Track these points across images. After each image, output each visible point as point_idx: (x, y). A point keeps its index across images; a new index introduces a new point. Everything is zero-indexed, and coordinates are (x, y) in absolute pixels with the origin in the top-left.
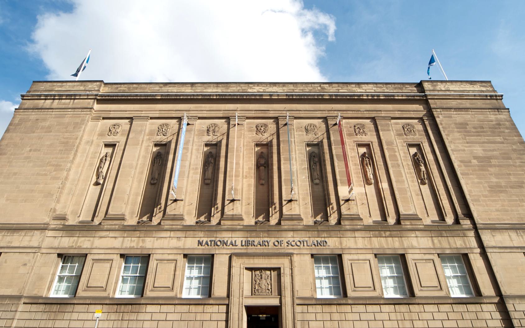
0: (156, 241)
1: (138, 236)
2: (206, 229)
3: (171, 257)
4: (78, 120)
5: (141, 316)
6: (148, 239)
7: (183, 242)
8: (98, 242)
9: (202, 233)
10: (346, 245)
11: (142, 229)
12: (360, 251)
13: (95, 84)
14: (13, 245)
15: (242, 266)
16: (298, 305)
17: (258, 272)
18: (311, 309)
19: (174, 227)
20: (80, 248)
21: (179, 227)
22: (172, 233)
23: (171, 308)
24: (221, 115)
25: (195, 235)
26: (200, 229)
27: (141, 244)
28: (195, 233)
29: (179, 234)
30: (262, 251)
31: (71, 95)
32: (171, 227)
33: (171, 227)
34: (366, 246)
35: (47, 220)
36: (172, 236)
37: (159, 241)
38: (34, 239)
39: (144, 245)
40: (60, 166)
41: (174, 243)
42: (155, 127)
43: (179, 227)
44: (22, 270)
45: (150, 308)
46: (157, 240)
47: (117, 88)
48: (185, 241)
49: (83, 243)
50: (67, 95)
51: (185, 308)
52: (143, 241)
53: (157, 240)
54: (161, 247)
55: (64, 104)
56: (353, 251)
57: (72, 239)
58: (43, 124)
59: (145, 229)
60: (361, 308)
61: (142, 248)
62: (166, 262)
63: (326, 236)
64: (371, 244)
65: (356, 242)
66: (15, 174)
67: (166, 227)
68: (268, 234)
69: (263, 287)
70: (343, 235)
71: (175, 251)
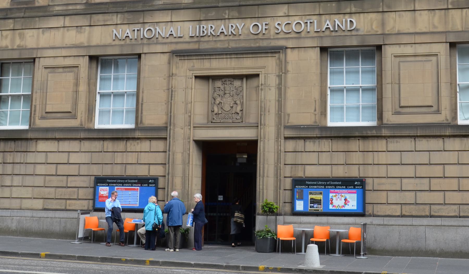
0: (41, 34)
1: (11, 27)
2: (126, 9)
5: (31, 158)
6: (29, 33)
7: (87, 32)
9: (119, 16)
10: (394, 27)
11: (17, 15)
12: (418, 39)
15: (190, 74)
16: (286, 138)
17: (218, 84)
18: (310, 146)
19: (70, 7)
21: (78, 7)
22: (67, 18)
23: (74, 146)
25: (107, 21)
26: (114, 10)
27: (18, 42)
28: (107, 17)
30: (226, 46)
32: (65, 8)
33: (65, 8)
34: (435, 27)
36: (67, 24)
37: (47, 34)
39: (22, 43)
41: (72, 37)
43: (78, 7)
45: (42, 146)
46: (43, 33)
48: (90, 33)
51: (97, 145)
52: (22, 37)
53: (43, 33)
54: (52, 45)
56: (406, 39)
59: (22, 15)
60: (406, 144)
61: (21, 49)
62: (61, 70)
63: (354, 10)
64: (446, 23)
65: (414, 21)
67: (57, 8)
68: (239, 12)
69: (227, 108)
70: (389, 7)
71: (74, 52)
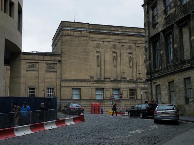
3: (126, 89)
4: (86, 42)
8: (105, 85)
13: (87, 25)
14: (83, 86)
20: (101, 87)
24: (133, 42)
27: (117, 86)
29: (127, 83)
31: (80, 30)
35: (89, 78)
38: (88, 84)
40: (87, 60)
41: (126, 86)
42: (111, 46)
44: (88, 93)
47: (94, 27)
49: (102, 85)
50: (79, 30)
52: (118, 85)
55: (79, 34)
57: (98, 84)
58: (74, 43)
66: (73, 63)
